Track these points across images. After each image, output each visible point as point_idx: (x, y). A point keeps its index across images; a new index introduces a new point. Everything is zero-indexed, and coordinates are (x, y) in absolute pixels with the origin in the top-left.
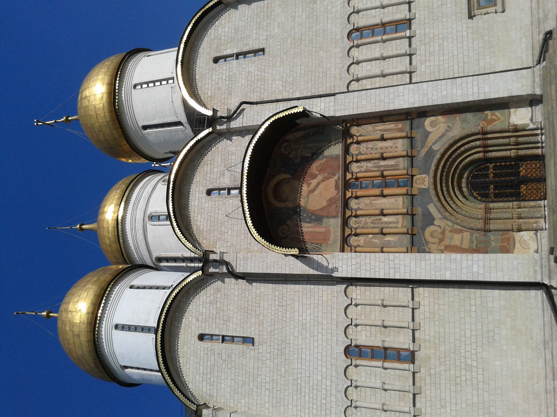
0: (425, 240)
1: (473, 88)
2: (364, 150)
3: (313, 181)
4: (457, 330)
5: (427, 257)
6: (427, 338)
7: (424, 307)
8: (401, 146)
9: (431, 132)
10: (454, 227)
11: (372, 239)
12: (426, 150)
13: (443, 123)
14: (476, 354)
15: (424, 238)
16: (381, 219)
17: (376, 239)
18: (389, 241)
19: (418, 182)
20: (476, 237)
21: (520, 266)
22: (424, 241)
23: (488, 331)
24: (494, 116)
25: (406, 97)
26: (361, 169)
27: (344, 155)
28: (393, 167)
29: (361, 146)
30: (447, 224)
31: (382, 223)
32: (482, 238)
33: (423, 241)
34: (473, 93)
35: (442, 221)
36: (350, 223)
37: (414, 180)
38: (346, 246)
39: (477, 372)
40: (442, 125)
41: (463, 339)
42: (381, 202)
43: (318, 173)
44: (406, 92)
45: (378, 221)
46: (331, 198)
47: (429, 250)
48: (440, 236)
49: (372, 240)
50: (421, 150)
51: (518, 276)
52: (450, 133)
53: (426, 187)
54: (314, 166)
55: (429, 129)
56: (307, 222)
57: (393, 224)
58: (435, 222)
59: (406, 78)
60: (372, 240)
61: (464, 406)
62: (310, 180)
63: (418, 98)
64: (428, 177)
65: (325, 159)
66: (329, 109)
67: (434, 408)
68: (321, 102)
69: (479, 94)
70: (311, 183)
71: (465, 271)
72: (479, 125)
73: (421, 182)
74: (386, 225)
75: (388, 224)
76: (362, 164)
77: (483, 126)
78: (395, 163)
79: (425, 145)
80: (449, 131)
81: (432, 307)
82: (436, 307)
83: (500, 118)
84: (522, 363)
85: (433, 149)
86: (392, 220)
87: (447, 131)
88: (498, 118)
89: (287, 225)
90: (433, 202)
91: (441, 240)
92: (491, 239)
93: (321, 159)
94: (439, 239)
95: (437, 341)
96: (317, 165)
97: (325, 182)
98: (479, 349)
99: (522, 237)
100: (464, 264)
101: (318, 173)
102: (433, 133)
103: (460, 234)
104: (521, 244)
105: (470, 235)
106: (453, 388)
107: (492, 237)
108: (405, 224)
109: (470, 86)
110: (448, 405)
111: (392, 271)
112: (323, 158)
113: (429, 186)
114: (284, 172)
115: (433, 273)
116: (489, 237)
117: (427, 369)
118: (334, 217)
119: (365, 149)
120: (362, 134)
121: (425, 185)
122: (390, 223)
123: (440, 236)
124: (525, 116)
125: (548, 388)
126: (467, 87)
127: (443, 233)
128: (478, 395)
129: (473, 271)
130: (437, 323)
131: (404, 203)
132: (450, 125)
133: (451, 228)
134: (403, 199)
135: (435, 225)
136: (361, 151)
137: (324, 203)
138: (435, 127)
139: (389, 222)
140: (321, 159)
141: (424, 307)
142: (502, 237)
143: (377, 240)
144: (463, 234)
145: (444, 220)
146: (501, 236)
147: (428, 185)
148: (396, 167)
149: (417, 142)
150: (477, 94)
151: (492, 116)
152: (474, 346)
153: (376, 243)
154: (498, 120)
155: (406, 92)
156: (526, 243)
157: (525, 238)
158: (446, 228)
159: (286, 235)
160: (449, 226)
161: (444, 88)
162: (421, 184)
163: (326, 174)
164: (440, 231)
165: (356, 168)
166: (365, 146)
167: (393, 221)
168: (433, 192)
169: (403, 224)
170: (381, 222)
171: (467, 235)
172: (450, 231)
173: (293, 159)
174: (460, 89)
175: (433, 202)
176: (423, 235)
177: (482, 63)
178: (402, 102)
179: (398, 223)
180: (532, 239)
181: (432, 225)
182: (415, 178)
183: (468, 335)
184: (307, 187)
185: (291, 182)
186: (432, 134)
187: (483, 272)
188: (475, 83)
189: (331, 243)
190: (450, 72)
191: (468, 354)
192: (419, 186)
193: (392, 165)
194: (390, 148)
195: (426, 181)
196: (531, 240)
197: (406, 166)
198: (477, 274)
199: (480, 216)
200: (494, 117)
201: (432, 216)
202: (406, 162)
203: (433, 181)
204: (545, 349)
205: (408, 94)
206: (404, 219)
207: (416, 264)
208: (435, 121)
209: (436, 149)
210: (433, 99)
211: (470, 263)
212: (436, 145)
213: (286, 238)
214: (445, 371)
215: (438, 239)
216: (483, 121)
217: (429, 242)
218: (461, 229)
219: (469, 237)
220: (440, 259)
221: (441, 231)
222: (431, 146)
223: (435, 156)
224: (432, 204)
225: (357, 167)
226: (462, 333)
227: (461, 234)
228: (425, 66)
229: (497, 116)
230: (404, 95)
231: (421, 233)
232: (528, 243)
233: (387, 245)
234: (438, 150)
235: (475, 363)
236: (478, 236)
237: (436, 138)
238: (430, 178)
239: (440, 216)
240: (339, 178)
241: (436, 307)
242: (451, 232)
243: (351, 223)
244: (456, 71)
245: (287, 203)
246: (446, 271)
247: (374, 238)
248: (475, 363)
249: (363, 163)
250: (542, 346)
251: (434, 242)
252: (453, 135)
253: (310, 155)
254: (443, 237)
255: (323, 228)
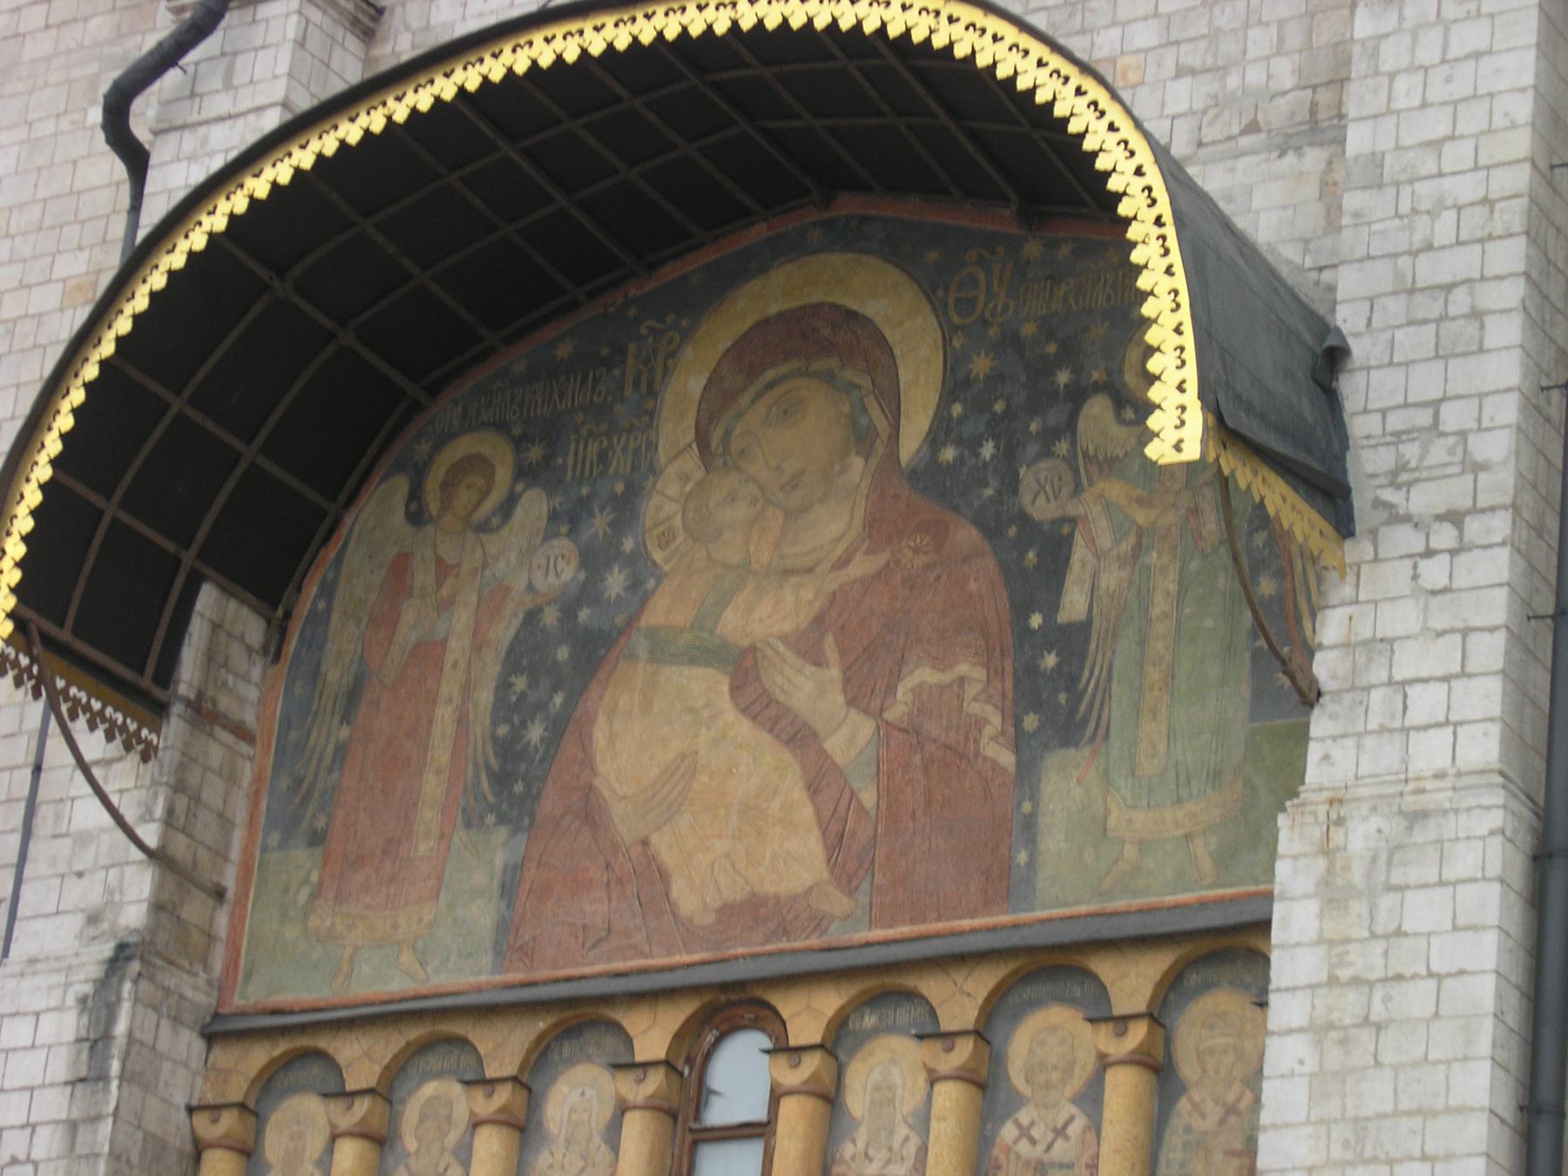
2: (1024, 1147)
3: (834, 673)
26: (862, 1135)
27: (1016, 939)
29: (1074, 1110)
36: (438, 1075)
38: (259, 1056)
43: (894, 713)
46: (664, 877)
54: (963, 668)
56: (504, 686)
62: (843, 653)
65: (1007, 759)
66: (1383, 730)
68: (1466, 632)
70: (819, 662)
76: (902, 1131)
89: (508, 506)
93: (1018, 724)
96: (971, 690)
97: (799, 794)
101: (894, 713)
112: (1019, 741)
114: (955, 385)
118: (504, 927)
119: (1039, 1150)
120: (1183, 1105)
136: (1024, 1116)
137: (625, 823)
140: (1018, 724)
159: (433, 506)
163: (868, 798)
165: (876, 1076)
166: (1061, 1150)
173: (1062, 447)
184: (787, 627)
185: (857, 464)
189: (314, 921)
213: (416, 517)
225: (884, 1097)
240: (819, 922)
243: (429, 1089)
245: (691, 462)
249: (914, 1141)
253: (1074, 604)
255: (442, 836)
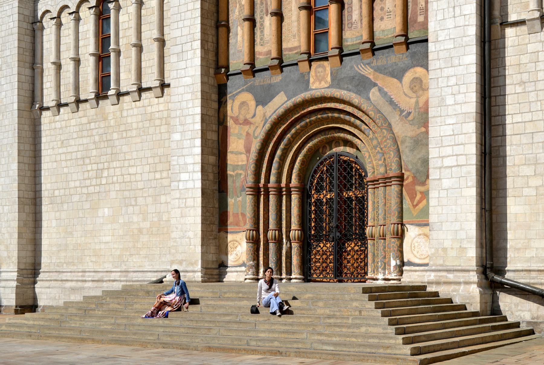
0: (237, 94)
1: (453, 156)
4: (134, 155)
5: (197, 101)
6: (125, 114)
7: (157, 104)
8: (383, 27)
9: (401, 82)
10: (254, 139)
11: (239, 5)
12: (371, 77)
13: (417, 102)
14: (113, 183)
15: (240, 92)
16: (267, 15)
17: (239, 12)
18: (237, 35)
19: (320, 70)
20: (241, 174)
21: (187, 240)
22: (234, 93)
23: (136, 198)
24: (421, 198)
25: (450, 23)
28: (348, 20)
30: (257, 127)
31: (261, 18)
32: (238, 184)
33: (235, 91)
34: (443, 157)
35: (262, 118)
37: (322, 62)
39: (97, 185)
40: (413, 101)
41: (126, 163)
42: (293, 9)
44: (461, 21)
45: (264, 11)
47: (224, 102)
48: (241, 118)
49: (238, 5)
50: (371, 68)
51: (176, 238)
52: (397, 117)
53: (311, 85)
55: (408, 77)
57: (260, 36)
58: (260, 107)
59: (519, 13)
60: (238, 5)
61: (66, 170)
63: (446, 47)
64: (326, 86)
67: (61, 132)
69: (440, 168)
71: (181, 161)
72: (407, 170)
73: (318, 74)
74: (258, 25)
75: (260, 29)
77: (405, 177)
78: (354, 20)
79: (380, 73)
80: (400, 115)
81: (157, 115)
82: (158, 122)
83: (417, 207)
84: (108, 243)
85: (371, 90)
86: (265, 36)
87: (402, 111)
88: (417, 205)
90: (289, 98)
91: (236, 120)
92: (238, 197)
94: (237, 117)
95: (122, 128)
98: (117, 187)
99: (240, 244)
100: (189, 160)
102: (400, 85)
103: (244, 150)
104: (232, 243)
105: (242, 166)
106: (79, 155)
107: (240, 199)
108: (261, 57)
109: (458, 150)
110: (64, 150)
111: (178, 49)
113: (314, 89)
115: (178, 113)
116: (241, 195)
117: (95, 117)
121: (314, 83)
122: (262, 32)
123: (241, 118)
124: (415, 252)
125: (87, 274)
126: (455, 145)
127: (246, 122)
128: (76, 187)
129: (182, 174)
130: (140, 125)
131: (291, 49)
132: (410, 118)
133: (252, 134)
134: (295, 48)
135: (257, 106)
138: (410, 87)
139: (264, 29)
141: (157, 104)
142: (240, 215)
143: (237, 14)
144: (243, 153)
145: (263, 122)
146: (242, 213)
147: (314, 88)
148: (348, 24)
149: (387, 57)
150: (439, 164)
151: (421, 193)
152: (120, 179)
153: (234, 12)
154: (413, 205)
155: (461, 21)
156: (232, 250)
157: (239, 248)
158: (252, 126)
160: (254, 131)
161: (460, 98)
162: (316, 76)
164: (249, 116)
167: (263, 35)
168: (299, 98)
169: (260, 54)
170: (264, 15)
171: (242, 161)
172: (248, 134)
174: (453, 131)
175: (289, 98)
176: (243, 90)
177: (528, 171)
178: (440, 17)
179: (262, 45)
180: (238, 257)
181: (256, 102)
182: (325, 63)
183: (132, 170)
186: (399, 84)
187: (180, 188)
188: (462, 160)
190: (518, 105)
191: (112, 171)
192: (312, 73)
193: (352, 17)
194: (380, 6)
195: (320, 83)
196: (236, 256)
197: (349, 43)
198: (178, 179)
199: (273, 178)
200: (418, 196)
201: (269, 102)
202: (355, 42)
203: (316, 96)
204: (120, 272)
205: (455, 27)
206: (267, 55)
207: (187, 85)
208: (421, 87)
209: (371, 95)
210: (440, 79)
211: (190, 168)
212: (378, 93)
214: (94, 143)
215: (237, 114)
216: (414, 177)
217: (233, 100)
218: (250, 151)
219: (240, 163)
220: (194, 123)
221: (248, 118)
222: (375, 85)
223: (360, 95)
224: (286, 99)
226: (132, 163)
227: (243, 150)
228: (538, 52)
229: (419, 202)
230: (454, 17)
231: (246, 86)
232: (233, 253)
233: (232, 33)
234: (368, 99)
235: (104, 181)
236: (242, 176)
237: (389, 94)
238: (323, 90)
239: (268, 114)
241: (158, 122)
242: (247, 135)
244: (517, 118)
246: (180, 134)
247: (240, 7)
248: (104, 181)
250: (124, 268)
251: (234, 109)
252: (393, 124)
254: (241, 122)
